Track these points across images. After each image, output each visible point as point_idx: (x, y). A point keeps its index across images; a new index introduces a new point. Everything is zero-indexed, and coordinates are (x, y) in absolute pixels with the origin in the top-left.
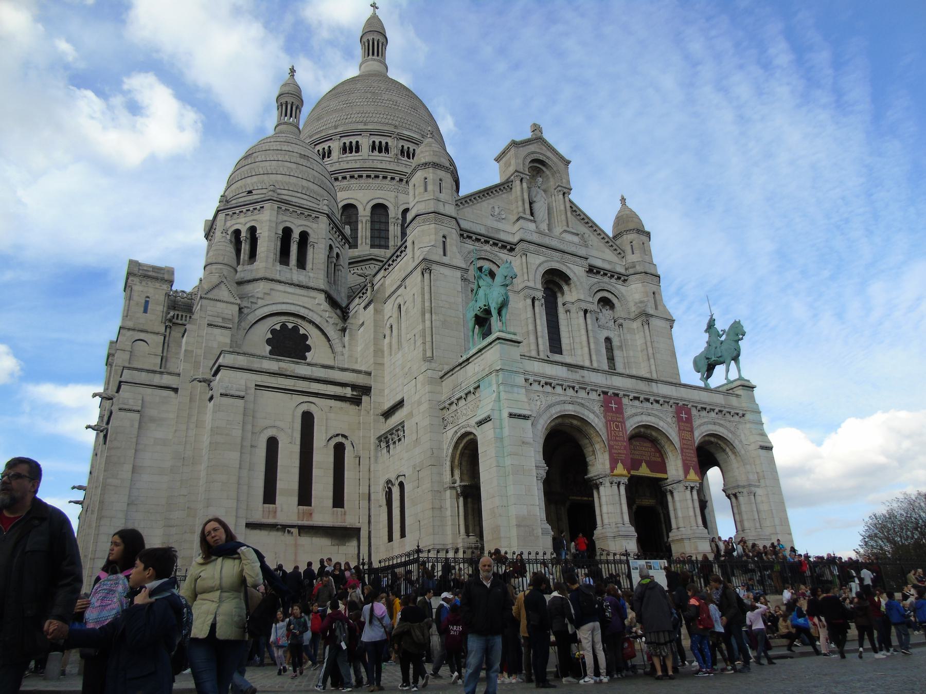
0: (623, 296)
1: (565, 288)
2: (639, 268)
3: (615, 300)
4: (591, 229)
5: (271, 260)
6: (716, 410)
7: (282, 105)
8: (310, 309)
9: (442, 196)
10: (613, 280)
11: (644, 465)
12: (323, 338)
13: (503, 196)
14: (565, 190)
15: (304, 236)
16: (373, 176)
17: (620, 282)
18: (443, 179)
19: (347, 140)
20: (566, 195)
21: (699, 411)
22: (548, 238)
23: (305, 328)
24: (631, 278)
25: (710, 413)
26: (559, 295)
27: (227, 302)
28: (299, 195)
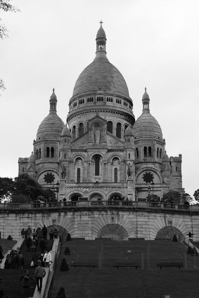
0: (121, 155)
1: (101, 158)
2: (126, 147)
5: (43, 157)
6: (118, 187)
8: (54, 169)
12: (58, 175)
14: (104, 130)
15: (52, 148)
16: (87, 112)
17: (121, 152)
19: (80, 99)
20: (105, 131)
23: (53, 173)
27: (33, 171)
28: (51, 137)
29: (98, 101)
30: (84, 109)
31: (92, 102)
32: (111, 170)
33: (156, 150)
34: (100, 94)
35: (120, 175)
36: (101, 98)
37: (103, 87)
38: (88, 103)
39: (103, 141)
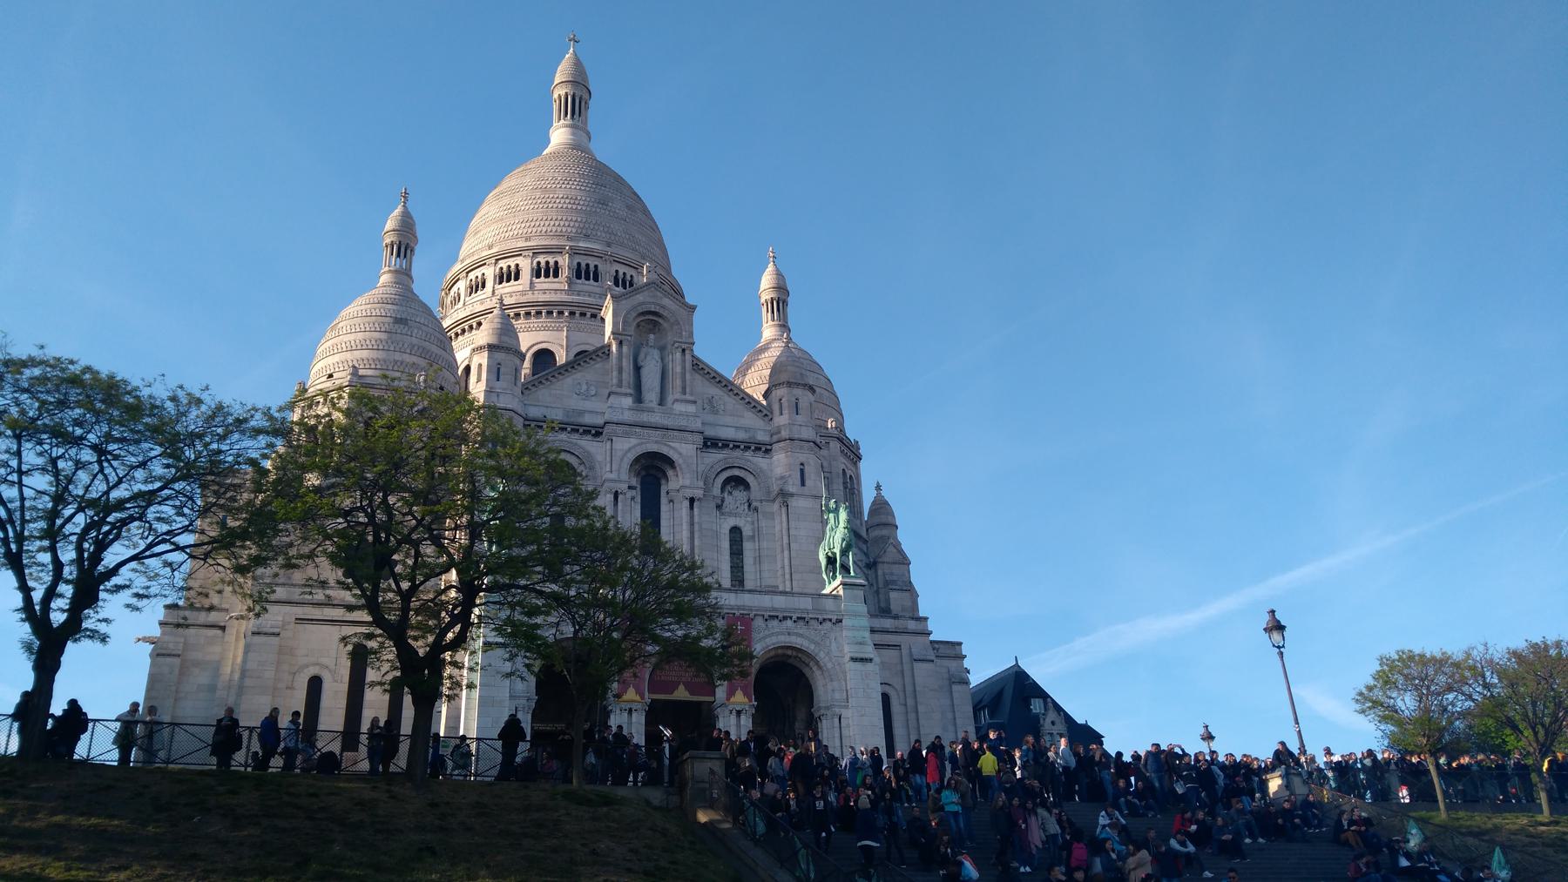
1: (670, 473)
3: (750, 479)
4: (725, 389)
6: (794, 618)
7: (387, 246)
9: (498, 386)
10: (748, 454)
11: (681, 687)
13: (597, 366)
14: (684, 346)
16: (533, 312)
18: (502, 363)
19: (503, 264)
20: (687, 352)
21: (766, 620)
22: (645, 414)
24: (775, 446)
25: (784, 622)
26: (663, 482)
29: (579, 277)
30: (523, 299)
31: (556, 280)
32: (717, 535)
33: (841, 480)
34: (588, 253)
35: (759, 560)
36: (592, 268)
37: (599, 234)
38: (538, 280)
39: (678, 396)
